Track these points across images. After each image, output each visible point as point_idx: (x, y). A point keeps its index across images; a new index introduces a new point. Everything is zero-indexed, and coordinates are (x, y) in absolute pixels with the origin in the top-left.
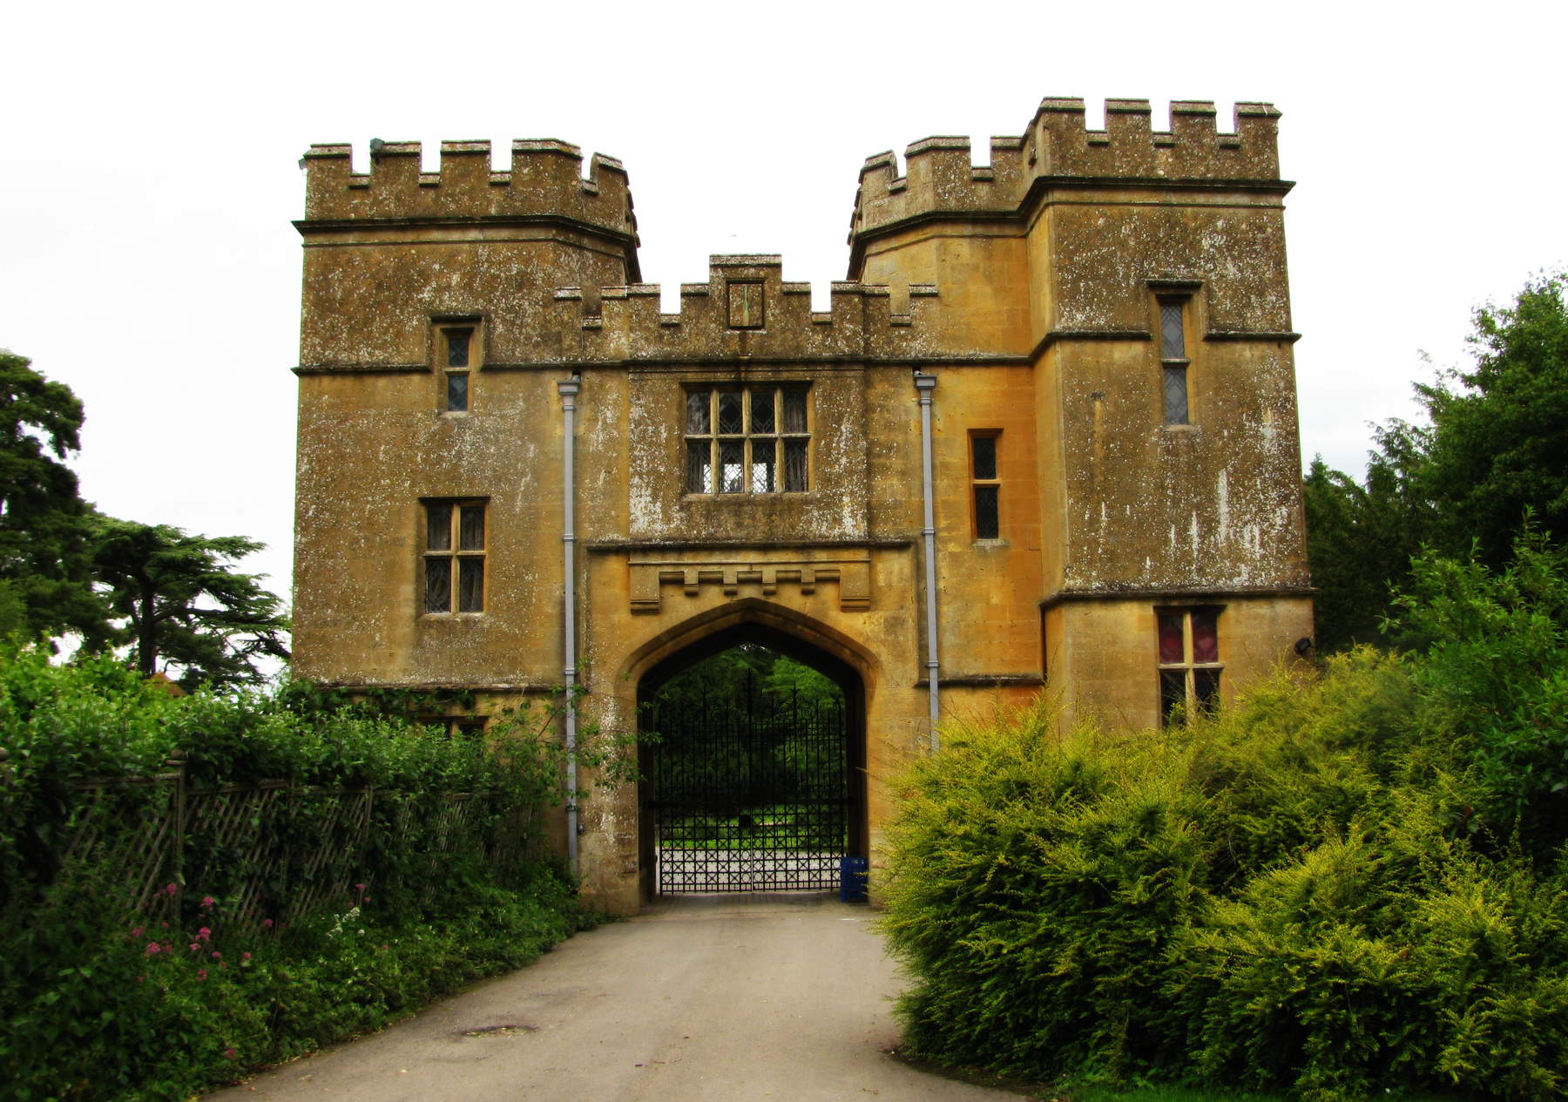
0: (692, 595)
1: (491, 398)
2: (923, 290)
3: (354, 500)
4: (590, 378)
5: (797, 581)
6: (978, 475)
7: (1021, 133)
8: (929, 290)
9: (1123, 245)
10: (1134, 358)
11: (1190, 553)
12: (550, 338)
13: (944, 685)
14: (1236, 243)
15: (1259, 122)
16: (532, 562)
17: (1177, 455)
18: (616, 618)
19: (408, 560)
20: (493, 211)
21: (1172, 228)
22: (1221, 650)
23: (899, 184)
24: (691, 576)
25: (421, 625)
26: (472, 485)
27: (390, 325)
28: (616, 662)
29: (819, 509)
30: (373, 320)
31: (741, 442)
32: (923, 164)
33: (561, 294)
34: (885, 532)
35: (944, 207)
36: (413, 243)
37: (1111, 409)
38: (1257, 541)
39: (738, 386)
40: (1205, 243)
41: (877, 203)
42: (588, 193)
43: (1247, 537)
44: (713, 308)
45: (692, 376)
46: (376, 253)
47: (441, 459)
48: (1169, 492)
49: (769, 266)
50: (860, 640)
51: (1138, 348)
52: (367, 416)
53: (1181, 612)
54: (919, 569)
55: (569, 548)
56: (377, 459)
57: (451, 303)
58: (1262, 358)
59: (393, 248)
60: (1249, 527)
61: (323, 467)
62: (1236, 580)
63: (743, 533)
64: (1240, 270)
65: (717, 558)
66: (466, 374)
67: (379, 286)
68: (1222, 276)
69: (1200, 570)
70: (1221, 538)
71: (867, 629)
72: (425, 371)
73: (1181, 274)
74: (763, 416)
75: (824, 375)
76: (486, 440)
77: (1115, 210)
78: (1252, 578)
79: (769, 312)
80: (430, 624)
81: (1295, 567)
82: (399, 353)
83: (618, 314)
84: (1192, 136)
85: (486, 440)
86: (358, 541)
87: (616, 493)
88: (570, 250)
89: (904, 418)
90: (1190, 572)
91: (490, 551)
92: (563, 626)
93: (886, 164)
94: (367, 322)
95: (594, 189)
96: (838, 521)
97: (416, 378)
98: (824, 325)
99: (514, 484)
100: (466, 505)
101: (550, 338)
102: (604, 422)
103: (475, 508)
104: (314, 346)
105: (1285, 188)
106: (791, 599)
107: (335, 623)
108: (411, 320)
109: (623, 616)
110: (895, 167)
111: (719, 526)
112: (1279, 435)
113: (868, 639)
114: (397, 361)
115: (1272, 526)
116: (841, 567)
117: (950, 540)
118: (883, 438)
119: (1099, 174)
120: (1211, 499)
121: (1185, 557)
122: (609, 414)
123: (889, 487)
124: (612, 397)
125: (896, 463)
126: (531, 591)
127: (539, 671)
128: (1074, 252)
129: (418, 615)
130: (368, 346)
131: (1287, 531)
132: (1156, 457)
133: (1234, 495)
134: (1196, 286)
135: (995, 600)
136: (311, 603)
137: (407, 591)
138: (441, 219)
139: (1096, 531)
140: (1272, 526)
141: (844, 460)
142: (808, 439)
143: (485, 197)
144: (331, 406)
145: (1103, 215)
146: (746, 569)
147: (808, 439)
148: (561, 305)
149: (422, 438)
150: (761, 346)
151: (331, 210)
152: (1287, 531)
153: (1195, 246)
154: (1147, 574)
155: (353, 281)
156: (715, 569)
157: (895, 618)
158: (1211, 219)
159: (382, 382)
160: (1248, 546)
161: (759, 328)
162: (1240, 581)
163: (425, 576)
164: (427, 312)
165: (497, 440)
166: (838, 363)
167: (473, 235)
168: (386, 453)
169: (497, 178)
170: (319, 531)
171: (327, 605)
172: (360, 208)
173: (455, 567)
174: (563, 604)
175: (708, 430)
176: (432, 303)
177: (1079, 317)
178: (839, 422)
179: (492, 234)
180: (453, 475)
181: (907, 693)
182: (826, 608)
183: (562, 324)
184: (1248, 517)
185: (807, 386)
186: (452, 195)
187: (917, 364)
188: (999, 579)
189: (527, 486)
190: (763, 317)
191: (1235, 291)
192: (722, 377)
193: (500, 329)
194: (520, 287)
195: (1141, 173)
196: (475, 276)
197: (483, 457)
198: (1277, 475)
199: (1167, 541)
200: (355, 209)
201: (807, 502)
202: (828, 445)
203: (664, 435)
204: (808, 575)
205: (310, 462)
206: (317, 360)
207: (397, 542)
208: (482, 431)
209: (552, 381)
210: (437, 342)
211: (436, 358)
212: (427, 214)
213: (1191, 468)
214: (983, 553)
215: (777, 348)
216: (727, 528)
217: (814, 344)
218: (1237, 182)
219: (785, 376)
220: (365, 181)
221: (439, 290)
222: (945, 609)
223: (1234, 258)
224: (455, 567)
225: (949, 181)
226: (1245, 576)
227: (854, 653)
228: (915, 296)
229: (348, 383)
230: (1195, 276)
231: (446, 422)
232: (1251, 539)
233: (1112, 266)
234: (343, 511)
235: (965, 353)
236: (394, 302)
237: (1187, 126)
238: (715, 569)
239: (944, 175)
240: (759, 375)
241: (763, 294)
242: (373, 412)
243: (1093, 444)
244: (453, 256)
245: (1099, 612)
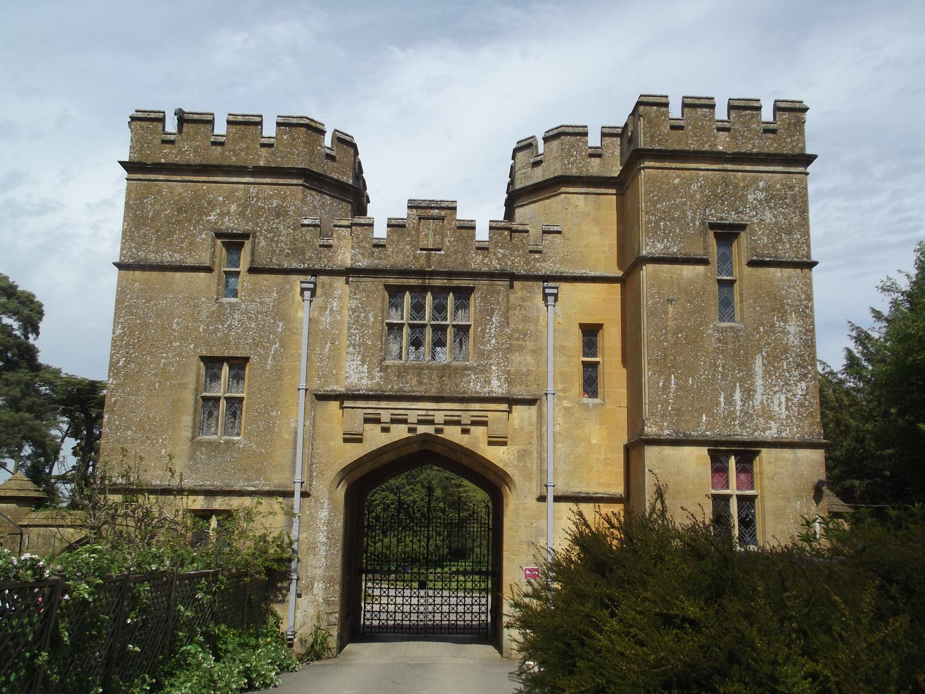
0: (385, 430)
1: (254, 290)
2: (552, 229)
3: (153, 355)
4: (322, 279)
5: (458, 423)
6: (585, 355)
7: (622, 125)
8: (556, 228)
9: (692, 197)
10: (697, 275)
11: (734, 412)
12: (297, 252)
13: (557, 499)
14: (772, 198)
15: (792, 114)
16: (277, 402)
17: (726, 343)
18: (332, 443)
19: (189, 398)
20: (262, 163)
21: (727, 186)
22: (757, 481)
23: (539, 158)
24: (385, 416)
25: (195, 444)
26: (237, 349)
27: (186, 237)
28: (332, 473)
29: (475, 374)
30: (174, 233)
31: (424, 326)
32: (555, 144)
33: (306, 222)
34: (519, 391)
35: (568, 173)
37: (680, 310)
38: (783, 406)
39: (424, 289)
40: (750, 197)
41: (523, 171)
42: (328, 156)
43: (776, 403)
44: (409, 235)
45: (392, 281)
46: (178, 188)
47: (217, 330)
48: (720, 369)
49: (448, 208)
50: (500, 465)
51: (701, 269)
52: (166, 298)
53: (728, 454)
54: (540, 414)
55: (303, 392)
56: (171, 328)
57: (231, 224)
58: (789, 277)
59: (191, 184)
60: (777, 395)
61: (132, 332)
62: (768, 432)
63: (422, 388)
64: (775, 216)
66: (238, 273)
67: (180, 210)
68: (762, 220)
69: (742, 424)
70: (757, 403)
71: (505, 457)
72: (209, 270)
73: (732, 218)
74: (440, 309)
75: (483, 284)
76: (249, 318)
77: (687, 173)
78: (779, 431)
79: (447, 240)
80: (201, 444)
81: (811, 425)
82: (191, 256)
83: (344, 237)
84: (743, 123)
85: (249, 318)
86: (154, 385)
87: (334, 358)
88: (314, 193)
89: (535, 314)
90: (734, 425)
91: (248, 395)
92: (295, 448)
93: (529, 146)
94: (170, 234)
95: (333, 153)
96: (488, 382)
97: (202, 275)
98: (483, 249)
100: (231, 362)
101: (297, 252)
102: (331, 310)
103: (238, 364)
104: (131, 248)
105: (810, 159)
106: (453, 434)
107: (133, 440)
108: (201, 234)
109: (338, 441)
110: (537, 147)
111: (407, 383)
112: (800, 331)
113: (506, 465)
114: (190, 262)
115: (794, 395)
116: (489, 414)
117: (565, 398)
118: (521, 327)
119: (677, 148)
120: (750, 376)
121: (731, 415)
122: (335, 304)
123: (522, 361)
124: (337, 293)
125: (530, 345)
126: (274, 423)
127: (276, 481)
128: (658, 201)
129: (193, 438)
130: (169, 250)
131: (805, 399)
132: (713, 344)
133: (767, 373)
134: (743, 227)
135: (594, 441)
136: (117, 426)
137: (187, 420)
138: (225, 166)
139: (667, 394)
140: (794, 395)
141: (493, 341)
142: (470, 326)
143: (256, 153)
144: (141, 290)
145: (678, 176)
146: (424, 413)
147: (470, 326)
148: (306, 228)
149: (204, 314)
150: (440, 262)
151: (148, 156)
152: (805, 399)
153: (743, 199)
154: (704, 427)
155: (161, 205)
156: (403, 412)
157: (524, 450)
158: (755, 181)
159: (178, 275)
160: (777, 409)
161: (440, 250)
162: (771, 434)
163: (200, 411)
164: (212, 229)
165: (257, 319)
166: (491, 275)
168: (178, 324)
169: (266, 141)
171: (129, 428)
172: (168, 155)
173: (223, 404)
174: (296, 433)
175: (402, 319)
176: (216, 223)
177: (660, 246)
178: (491, 315)
180: (225, 342)
181: (532, 502)
182: (477, 441)
183: (305, 241)
184: (777, 389)
185: (471, 290)
186: (233, 151)
187: (546, 278)
188: (598, 426)
189: (276, 351)
190: (442, 243)
191: (771, 231)
192: (413, 282)
193: (263, 243)
194: (278, 216)
195: (707, 148)
196: (248, 206)
197: (246, 330)
198: (799, 360)
199: (718, 404)
201: (466, 368)
202: (483, 330)
203: (372, 320)
204: (466, 418)
205: (123, 328)
206: (133, 258)
207: (183, 386)
208: (247, 312)
209: (296, 279)
210: (218, 250)
211: (217, 261)
212: (215, 163)
213: (736, 353)
214: (586, 407)
216: (411, 385)
217: (477, 262)
218: (775, 155)
219: (456, 283)
220: (172, 138)
221: (222, 215)
222: (559, 445)
223: (770, 208)
224: (223, 404)
225: (572, 156)
226: (775, 431)
227: (496, 474)
228: (544, 232)
230: (742, 220)
231: (221, 305)
232: (779, 405)
233: (684, 212)
235: (579, 272)
236: (190, 221)
237: (741, 116)
238: (403, 412)
239: (569, 151)
240: (438, 282)
241: (442, 228)
242: (171, 296)
243: (666, 334)
244: (233, 192)
245: (668, 450)
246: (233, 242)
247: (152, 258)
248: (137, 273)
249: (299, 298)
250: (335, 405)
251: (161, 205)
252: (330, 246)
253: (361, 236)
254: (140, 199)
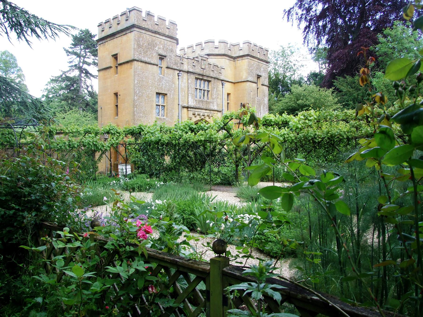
4: (181, 72)
12: (176, 64)
24: (196, 114)
45: (197, 77)
65: (200, 110)
72: (157, 65)
75: (212, 80)
94: (147, 52)
97: (155, 66)
101: (176, 64)
114: (152, 62)
124: (185, 77)
144: (141, 69)
164: (157, 53)
166: (215, 78)
170: (139, 96)
187: (222, 80)
193: (168, 60)
200: (144, 25)
208: (166, 80)
215: (207, 74)
216: (201, 106)
217: (212, 74)
219: (208, 79)
229: (143, 64)
234: (143, 93)
235: (227, 80)
240: (205, 78)
246: (162, 57)
247: (143, 59)
248: (140, 63)
249: (177, 77)
250: (185, 110)
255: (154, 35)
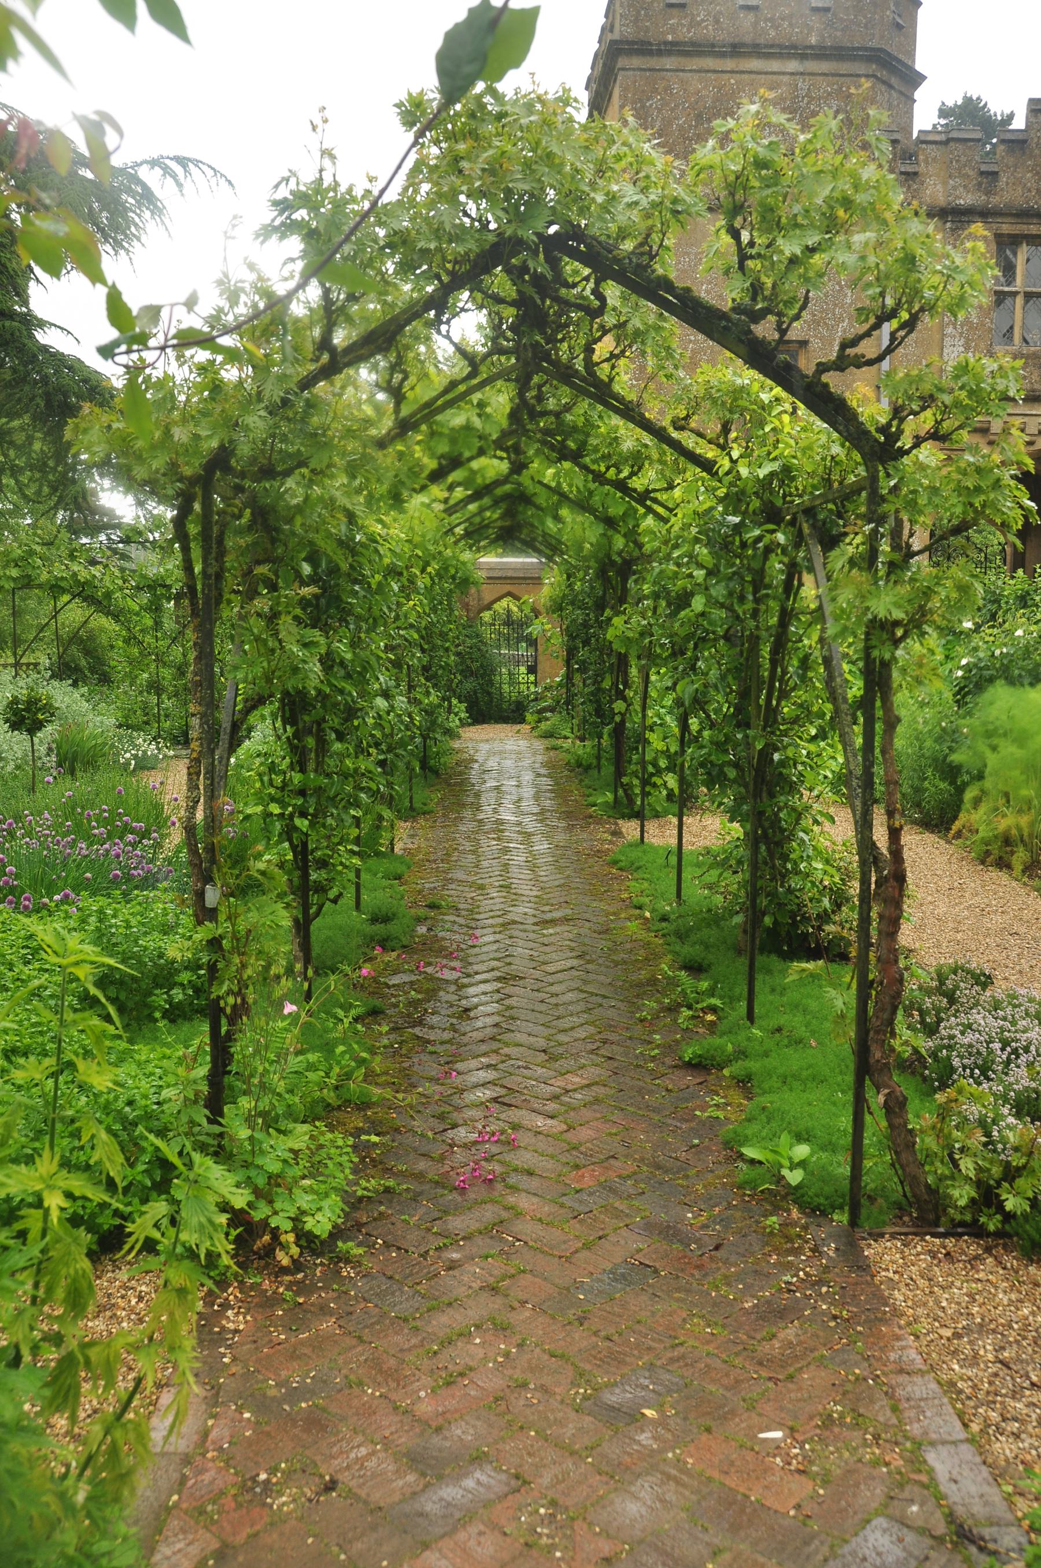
20: (813, 40)
36: (732, 72)
45: (1006, 229)
52: (688, 254)
59: (713, 76)
83: (934, 159)
99: (832, 329)
155: (672, 110)
167: (793, 65)
179: (812, 66)
200: (673, 30)
251: (672, 110)
252: (916, 174)
253: (963, 159)
254: (640, 100)
255: (729, 64)
